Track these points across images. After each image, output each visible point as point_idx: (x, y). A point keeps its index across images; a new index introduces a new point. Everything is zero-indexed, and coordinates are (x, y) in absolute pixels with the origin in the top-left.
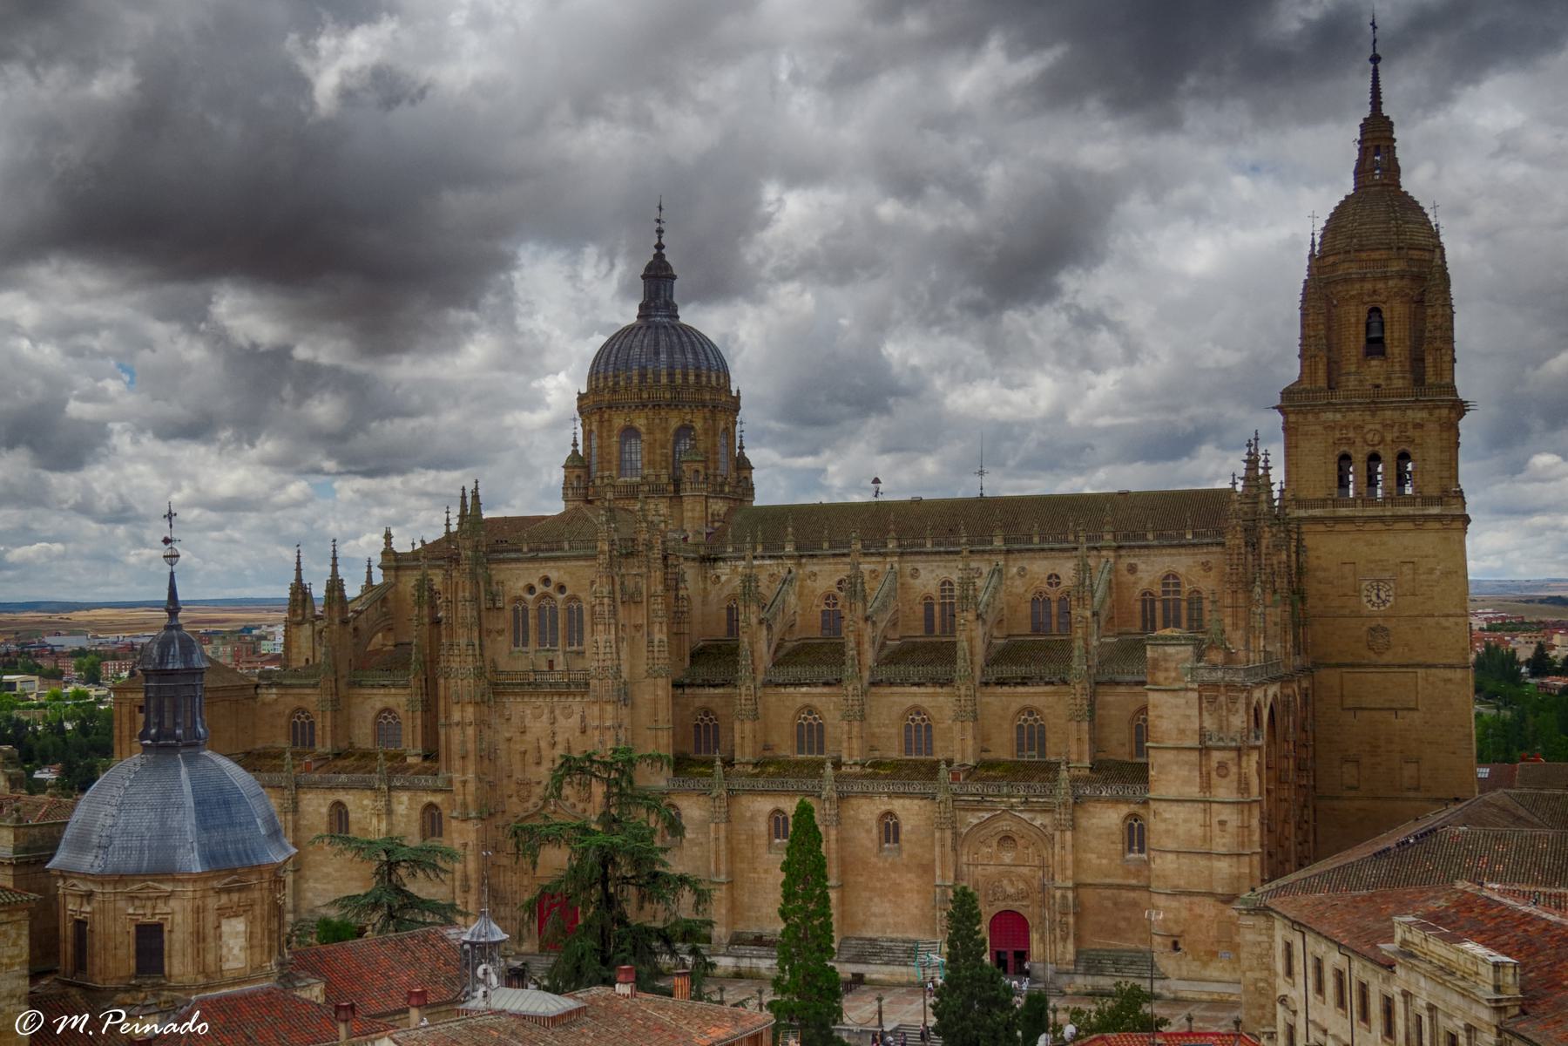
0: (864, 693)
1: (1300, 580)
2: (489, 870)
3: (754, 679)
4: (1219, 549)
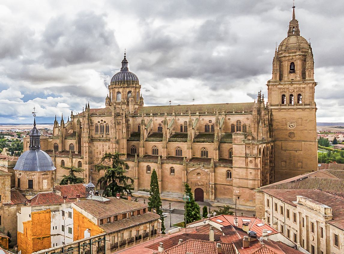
0: (167, 143)
1: (271, 122)
2: (91, 174)
3: (144, 140)
4: (251, 115)
